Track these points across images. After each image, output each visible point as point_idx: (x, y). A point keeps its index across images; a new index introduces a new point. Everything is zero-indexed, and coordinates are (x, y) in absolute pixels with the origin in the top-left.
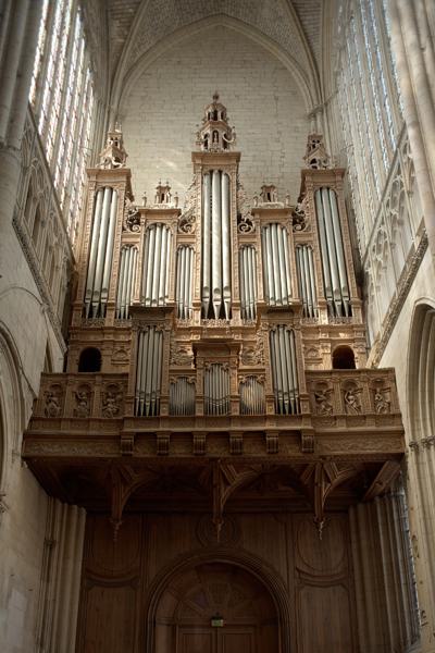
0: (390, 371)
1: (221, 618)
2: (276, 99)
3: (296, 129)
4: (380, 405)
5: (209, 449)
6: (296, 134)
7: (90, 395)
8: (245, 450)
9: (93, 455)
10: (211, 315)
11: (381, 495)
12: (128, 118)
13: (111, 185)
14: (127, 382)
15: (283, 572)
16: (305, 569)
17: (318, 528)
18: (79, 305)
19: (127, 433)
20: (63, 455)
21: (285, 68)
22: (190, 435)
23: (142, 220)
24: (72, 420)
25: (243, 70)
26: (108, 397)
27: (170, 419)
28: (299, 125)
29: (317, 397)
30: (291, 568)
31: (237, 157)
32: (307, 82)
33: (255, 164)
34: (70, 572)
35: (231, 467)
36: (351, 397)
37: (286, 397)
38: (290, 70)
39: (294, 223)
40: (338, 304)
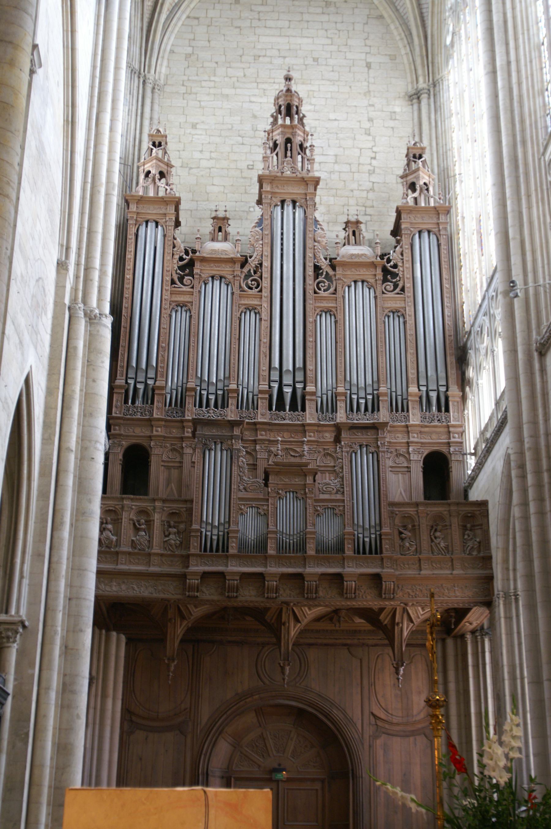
0: (484, 504)
1: (284, 770)
2: (369, 66)
3: (393, 116)
4: (470, 544)
5: (281, 592)
6: (392, 124)
7: (149, 523)
8: (321, 594)
9: (155, 595)
10: (281, 406)
11: (473, 632)
12: (168, 89)
13: (154, 217)
14: (192, 509)
15: (356, 716)
16: (382, 715)
17: (397, 673)
18: (120, 387)
19: (195, 573)
20: (123, 594)
21: (381, 17)
22: (261, 576)
23: (195, 271)
24: (130, 553)
25: (325, 18)
26: (170, 526)
27: (241, 557)
28: (397, 109)
29: (401, 533)
30: (366, 713)
31: (316, 182)
32: (411, 43)
33: (337, 167)
34: (109, 714)
35: (306, 608)
36: (438, 534)
37: (367, 534)
38: (389, 21)
39: (385, 280)
40: (433, 395)
